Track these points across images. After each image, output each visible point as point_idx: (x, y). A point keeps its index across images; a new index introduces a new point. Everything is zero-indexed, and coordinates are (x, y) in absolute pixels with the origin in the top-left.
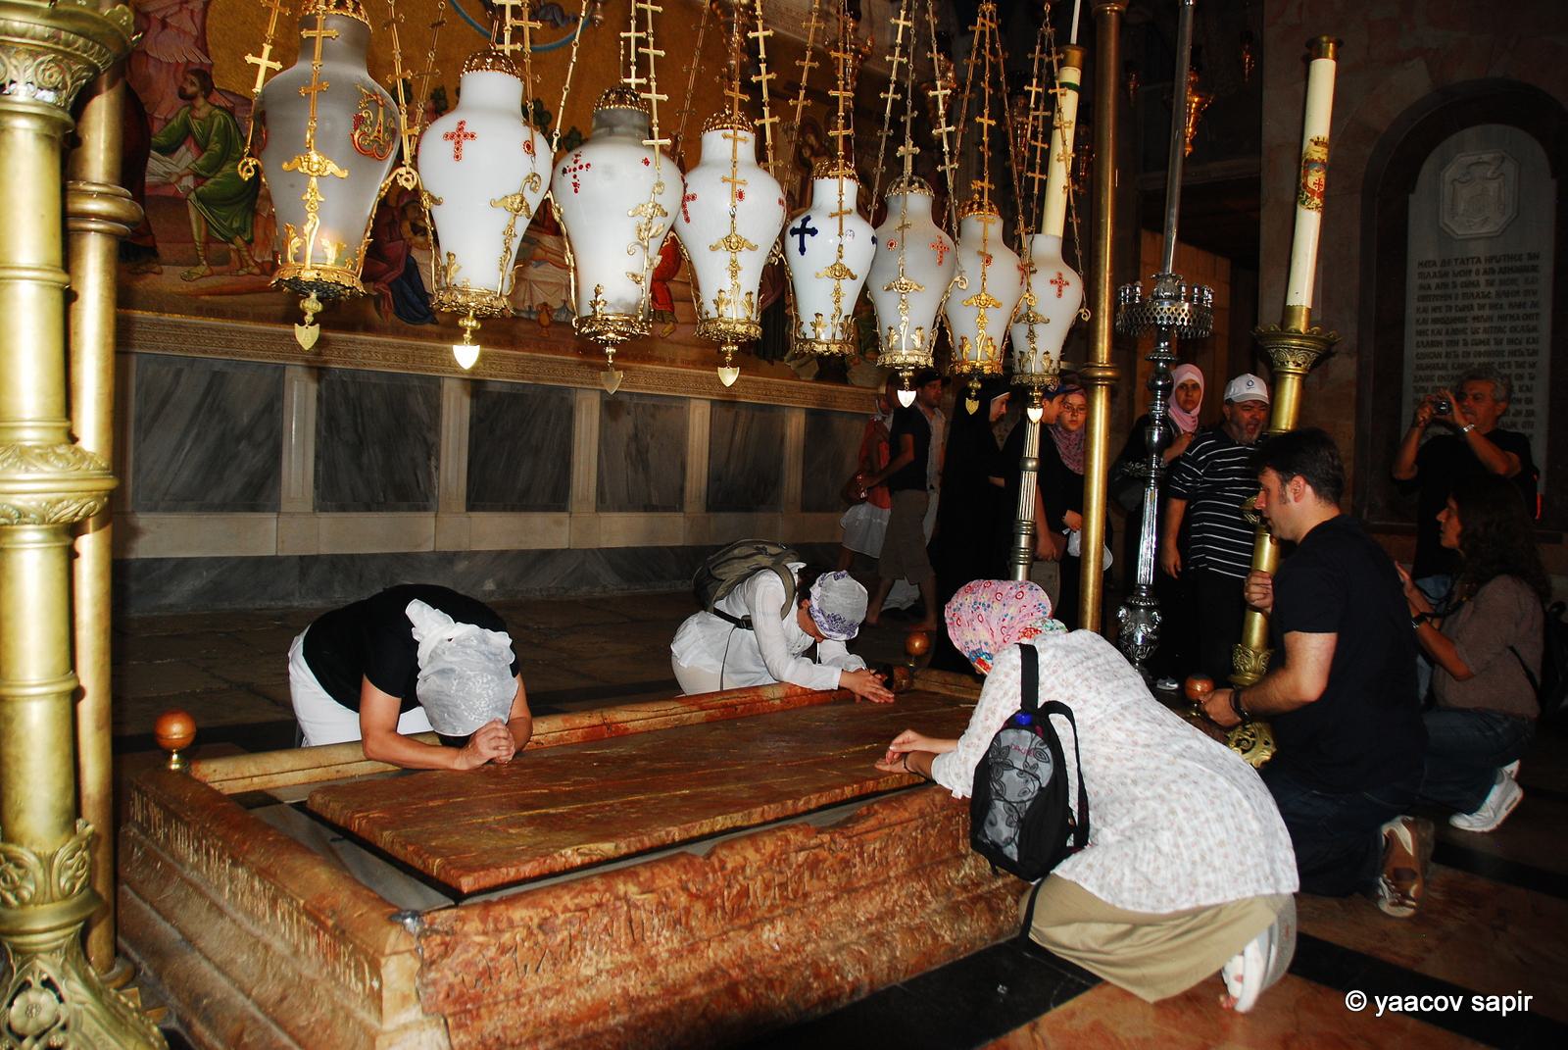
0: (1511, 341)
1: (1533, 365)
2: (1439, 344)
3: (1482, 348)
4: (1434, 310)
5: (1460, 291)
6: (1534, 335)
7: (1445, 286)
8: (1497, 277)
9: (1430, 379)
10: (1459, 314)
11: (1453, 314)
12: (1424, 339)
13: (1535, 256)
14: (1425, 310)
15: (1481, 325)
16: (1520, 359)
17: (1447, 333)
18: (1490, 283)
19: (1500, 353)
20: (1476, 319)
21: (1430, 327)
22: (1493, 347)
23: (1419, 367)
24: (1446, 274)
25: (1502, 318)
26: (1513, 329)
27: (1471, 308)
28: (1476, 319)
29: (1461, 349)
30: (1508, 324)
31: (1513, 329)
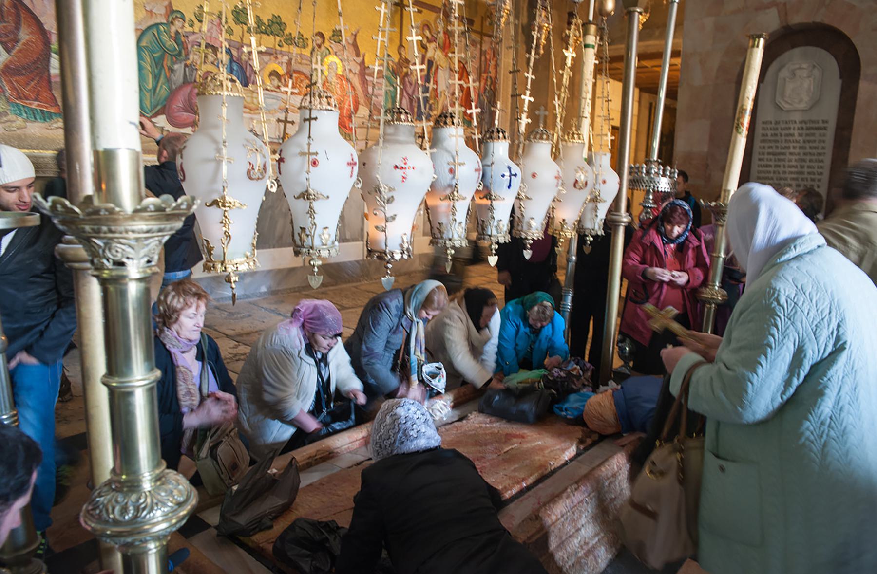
0: (809, 167)
1: (819, 180)
2: (770, 166)
3: (793, 170)
4: (770, 147)
5: (783, 138)
6: (821, 164)
7: (776, 135)
8: (804, 132)
10: (783, 151)
11: (779, 151)
12: (762, 163)
13: (827, 122)
14: (764, 148)
15: (793, 157)
16: (813, 177)
17: (775, 161)
18: (800, 135)
19: (802, 173)
20: (791, 154)
21: (766, 157)
22: (799, 169)
24: (777, 129)
25: (805, 154)
26: (811, 161)
27: (788, 148)
28: (791, 154)
29: (782, 169)
30: (808, 158)
31: (811, 161)
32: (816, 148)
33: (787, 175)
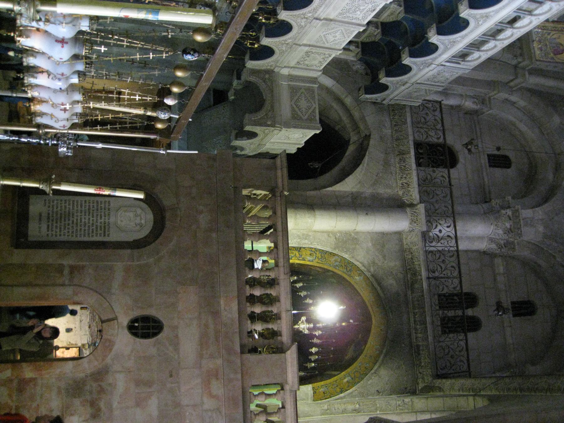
2: (81, 207)
3: (79, 221)
5: (99, 214)
6: (82, 236)
7: (101, 209)
8: (103, 225)
9: (69, 205)
11: (91, 212)
13: (108, 236)
14: (93, 203)
21: (87, 204)
23: (73, 201)
24: (105, 209)
26: (85, 230)
27: (93, 217)
28: (89, 219)
29: (79, 214)
32: (93, 232)
33: (75, 218)
